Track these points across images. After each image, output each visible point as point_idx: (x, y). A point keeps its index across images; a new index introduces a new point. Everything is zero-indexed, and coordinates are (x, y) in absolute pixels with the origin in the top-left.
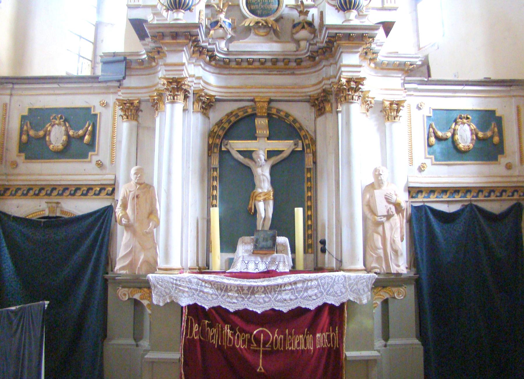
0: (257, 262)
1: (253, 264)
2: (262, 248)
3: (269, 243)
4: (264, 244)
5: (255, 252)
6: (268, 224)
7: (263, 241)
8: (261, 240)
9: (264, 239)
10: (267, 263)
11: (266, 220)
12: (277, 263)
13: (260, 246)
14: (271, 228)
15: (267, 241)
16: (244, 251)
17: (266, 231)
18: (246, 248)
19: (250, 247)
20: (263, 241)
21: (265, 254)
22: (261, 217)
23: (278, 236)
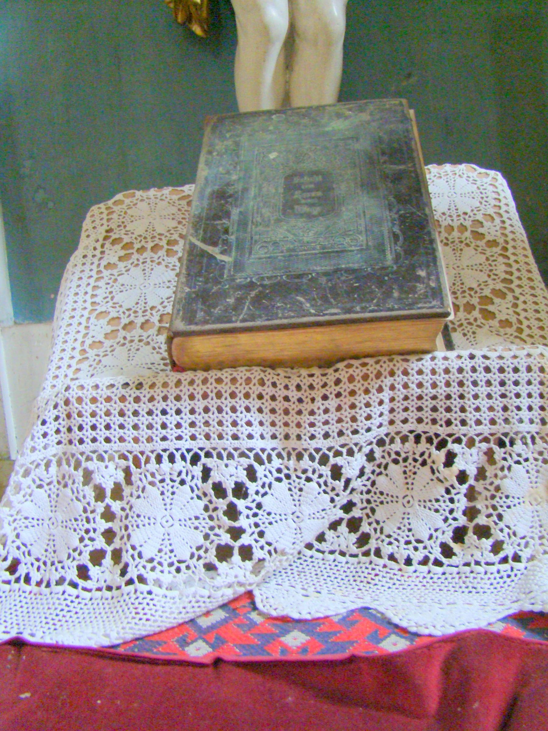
0: (229, 473)
1: (188, 504)
2: (271, 295)
3: (360, 225)
4: (301, 234)
5: (203, 347)
6: (322, 76)
7: (288, 208)
8: (260, 198)
9: (291, 184)
10: (352, 466)
11: (306, 54)
12: (468, 460)
13: (257, 266)
14: (347, 92)
15: (327, 200)
16: (99, 329)
17: (313, 113)
18: (127, 299)
19: (158, 285)
20: (288, 208)
21: (327, 362)
22: (265, 31)
23: (426, 164)
